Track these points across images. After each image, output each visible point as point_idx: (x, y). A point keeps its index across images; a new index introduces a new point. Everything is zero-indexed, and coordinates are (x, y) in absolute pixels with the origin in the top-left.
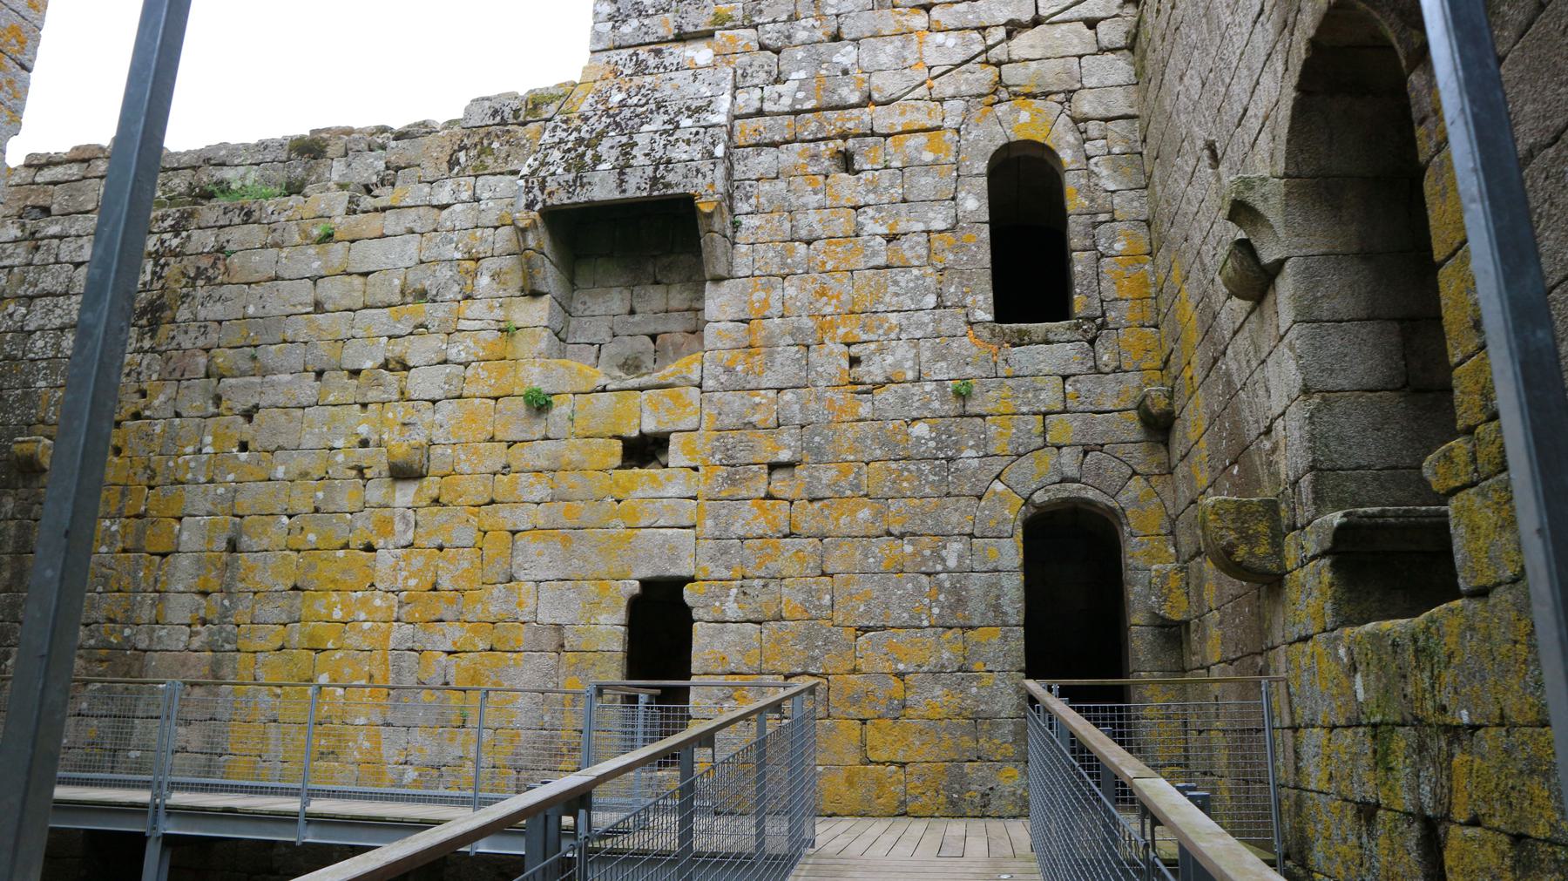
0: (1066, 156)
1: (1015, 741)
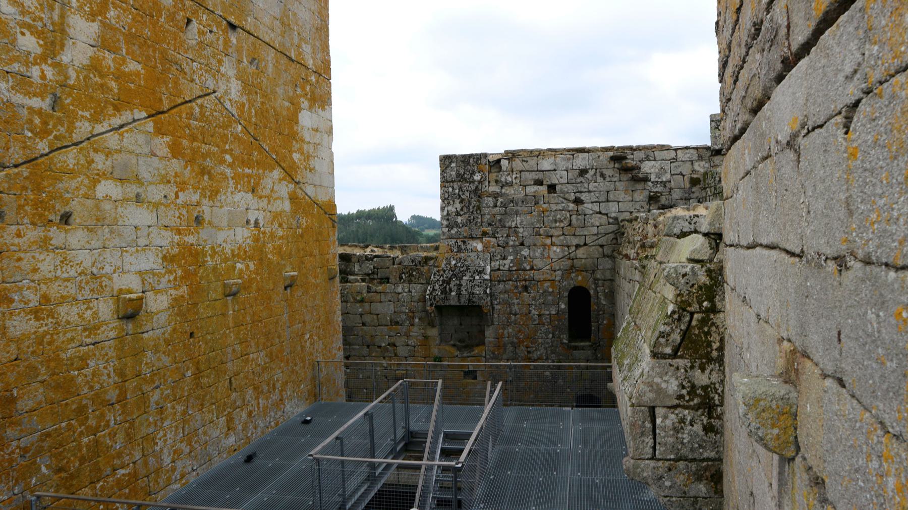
0: (592, 292)
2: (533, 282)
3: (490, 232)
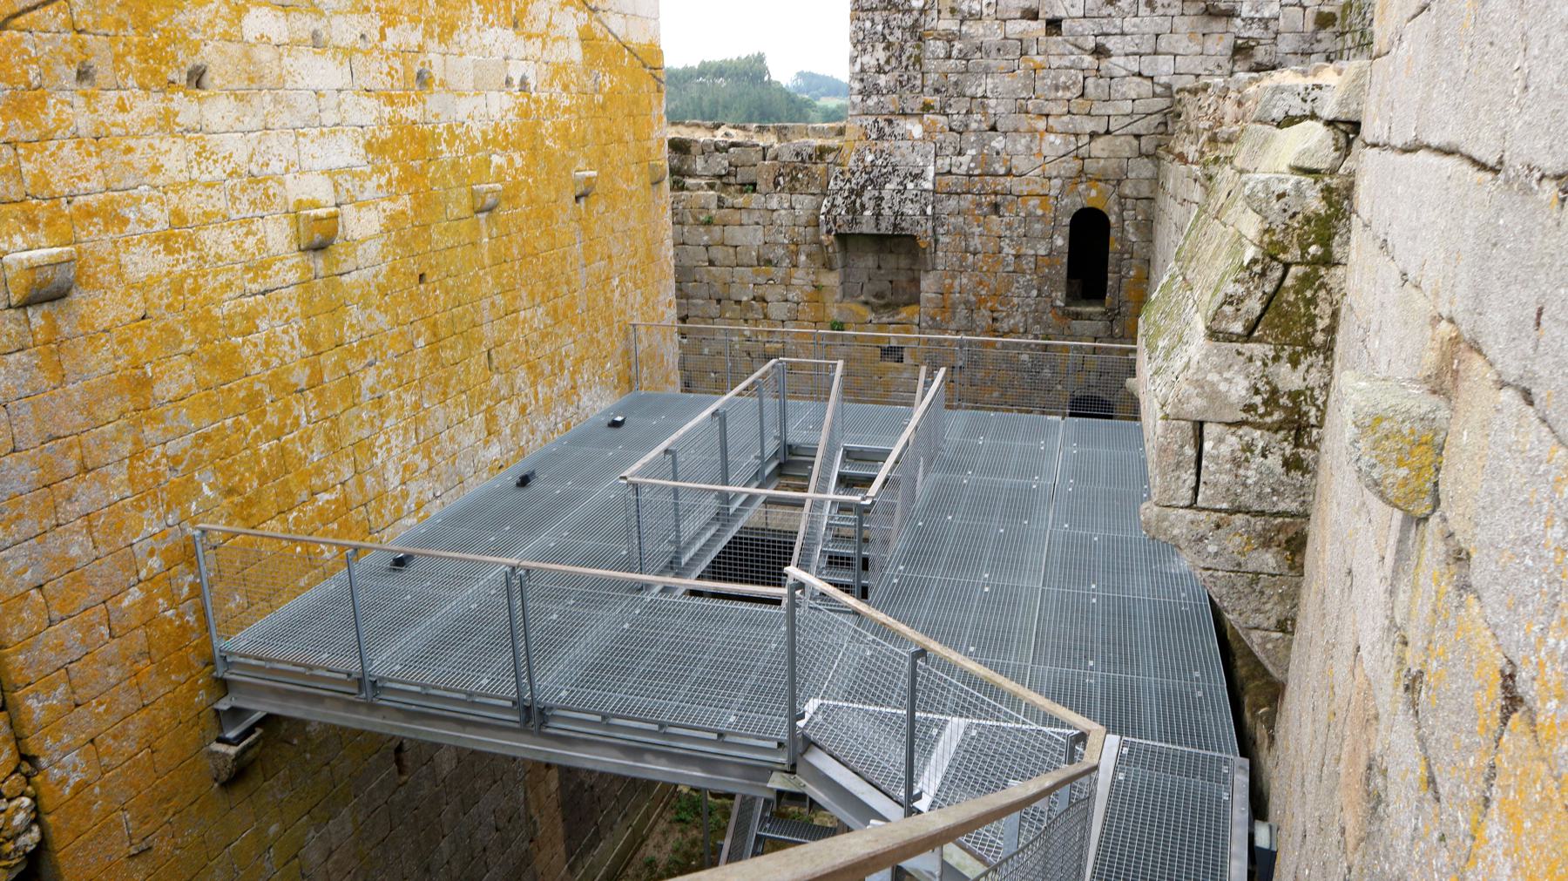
0: (1113, 219)
2: (1009, 197)
3: (937, 105)
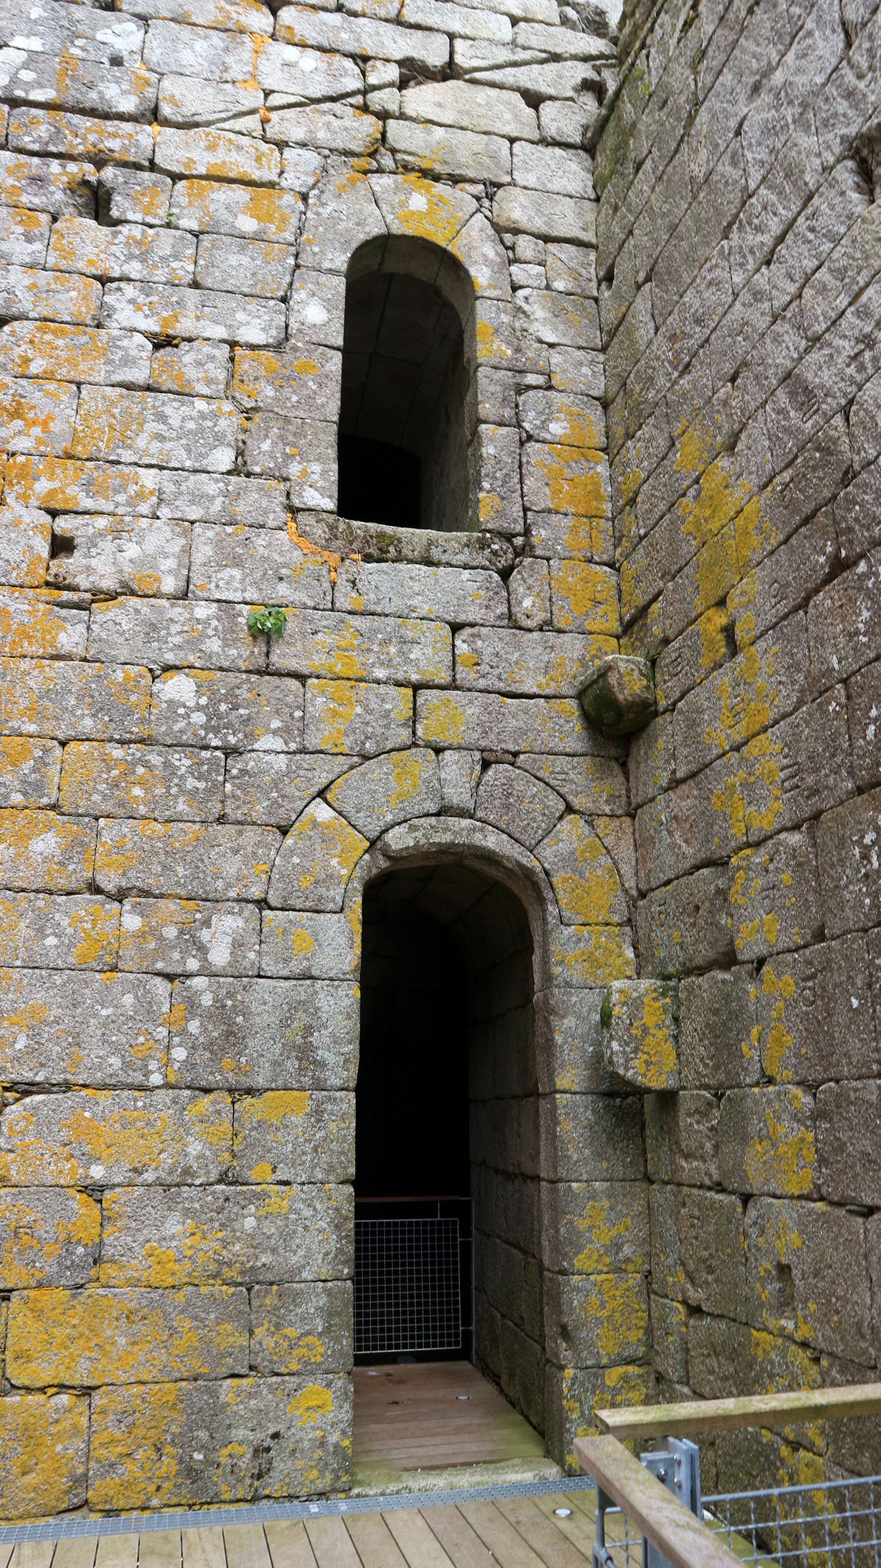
1: (327, 1330)
